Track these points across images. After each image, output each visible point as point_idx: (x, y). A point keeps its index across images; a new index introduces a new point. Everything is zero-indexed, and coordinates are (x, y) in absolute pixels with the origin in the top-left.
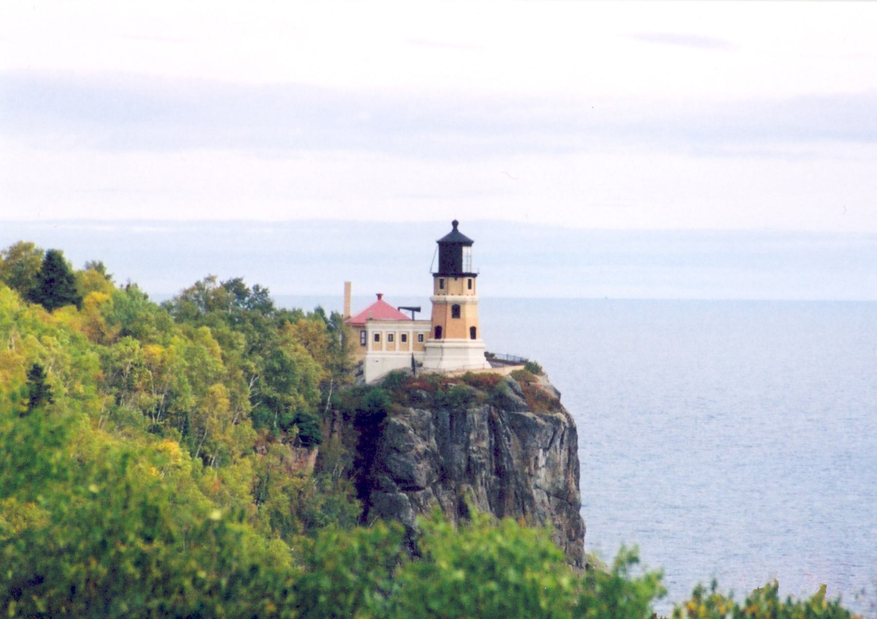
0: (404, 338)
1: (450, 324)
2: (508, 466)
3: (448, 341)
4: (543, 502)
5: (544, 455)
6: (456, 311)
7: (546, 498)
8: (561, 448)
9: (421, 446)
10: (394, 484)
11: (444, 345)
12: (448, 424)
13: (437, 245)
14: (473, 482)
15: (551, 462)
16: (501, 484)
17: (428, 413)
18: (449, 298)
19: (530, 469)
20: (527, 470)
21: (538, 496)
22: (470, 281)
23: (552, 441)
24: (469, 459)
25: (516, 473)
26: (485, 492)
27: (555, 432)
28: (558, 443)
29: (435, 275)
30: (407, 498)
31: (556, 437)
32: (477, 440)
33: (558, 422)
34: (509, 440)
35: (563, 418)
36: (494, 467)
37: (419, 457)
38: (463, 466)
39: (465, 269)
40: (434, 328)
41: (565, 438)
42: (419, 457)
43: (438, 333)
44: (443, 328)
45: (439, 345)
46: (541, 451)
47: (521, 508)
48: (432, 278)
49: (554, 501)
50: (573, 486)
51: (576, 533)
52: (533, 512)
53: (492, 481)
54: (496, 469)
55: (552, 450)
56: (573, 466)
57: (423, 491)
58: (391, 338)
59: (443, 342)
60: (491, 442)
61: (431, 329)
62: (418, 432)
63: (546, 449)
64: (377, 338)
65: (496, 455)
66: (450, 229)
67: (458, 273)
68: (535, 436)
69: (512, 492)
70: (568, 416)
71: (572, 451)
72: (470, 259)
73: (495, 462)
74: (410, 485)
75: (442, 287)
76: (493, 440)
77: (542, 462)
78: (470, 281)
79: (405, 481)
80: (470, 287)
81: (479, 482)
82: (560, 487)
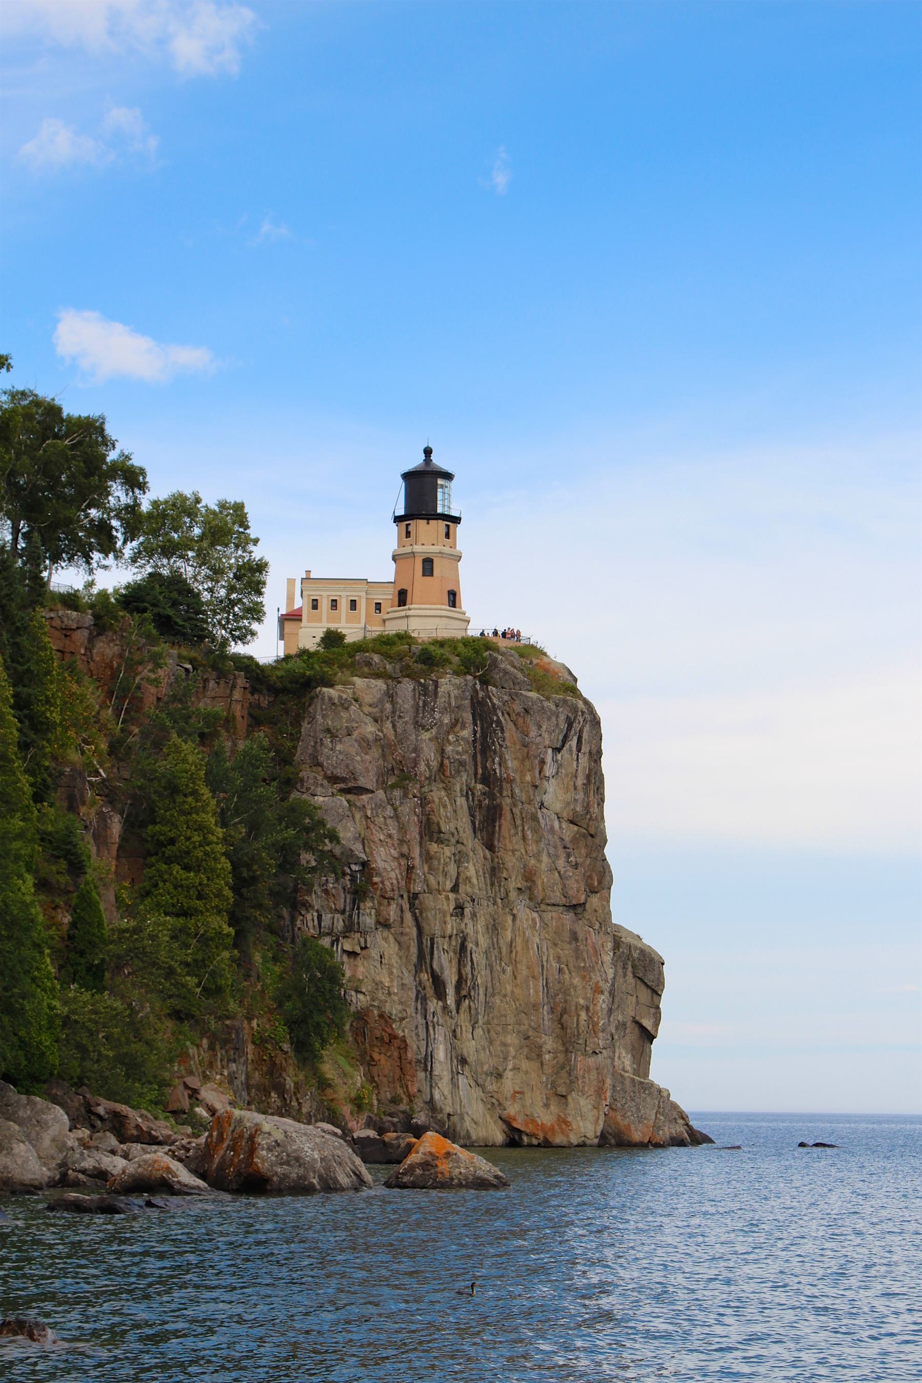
0: (353, 605)
1: (420, 585)
2: (500, 771)
3: (413, 608)
4: (552, 827)
5: (555, 761)
6: (428, 566)
7: (556, 825)
8: (579, 750)
9: (369, 729)
10: (325, 782)
15: (563, 771)
16: (491, 795)
17: (380, 685)
18: (418, 548)
20: (528, 778)
21: (547, 819)
22: (448, 526)
23: (565, 739)
25: (511, 781)
26: (465, 807)
28: (574, 742)
29: (398, 519)
31: (573, 732)
33: (575, 709)
35: (581, 704)
36: (480, 771)
37: (365, 744)
38: (435, 764)
39: (440, 510)
40: (397, 593)
41: (585, 736)
43: (402, 598)
45: (403, 614)
46: (550, 751)
47: (520, 834)
49: (569, 831)
50: (595, 809)
51: (600, 882)
52: (538, 842)
53: (478, 793)
54: (483, 774)
57: (370, 795)
58: (334, 604)
59: (410, 609)
60: (475, 732)
61: (393, 595)
62: (367, 709)
67: (433, 515)
69: (508, 808)
70: (586, 702)
71: (596, 755)
73: (482, 763)
74: (350, 785)
78: (448, 526)
79: (343, 780)
80: (447, 536)
82: (578, 809)
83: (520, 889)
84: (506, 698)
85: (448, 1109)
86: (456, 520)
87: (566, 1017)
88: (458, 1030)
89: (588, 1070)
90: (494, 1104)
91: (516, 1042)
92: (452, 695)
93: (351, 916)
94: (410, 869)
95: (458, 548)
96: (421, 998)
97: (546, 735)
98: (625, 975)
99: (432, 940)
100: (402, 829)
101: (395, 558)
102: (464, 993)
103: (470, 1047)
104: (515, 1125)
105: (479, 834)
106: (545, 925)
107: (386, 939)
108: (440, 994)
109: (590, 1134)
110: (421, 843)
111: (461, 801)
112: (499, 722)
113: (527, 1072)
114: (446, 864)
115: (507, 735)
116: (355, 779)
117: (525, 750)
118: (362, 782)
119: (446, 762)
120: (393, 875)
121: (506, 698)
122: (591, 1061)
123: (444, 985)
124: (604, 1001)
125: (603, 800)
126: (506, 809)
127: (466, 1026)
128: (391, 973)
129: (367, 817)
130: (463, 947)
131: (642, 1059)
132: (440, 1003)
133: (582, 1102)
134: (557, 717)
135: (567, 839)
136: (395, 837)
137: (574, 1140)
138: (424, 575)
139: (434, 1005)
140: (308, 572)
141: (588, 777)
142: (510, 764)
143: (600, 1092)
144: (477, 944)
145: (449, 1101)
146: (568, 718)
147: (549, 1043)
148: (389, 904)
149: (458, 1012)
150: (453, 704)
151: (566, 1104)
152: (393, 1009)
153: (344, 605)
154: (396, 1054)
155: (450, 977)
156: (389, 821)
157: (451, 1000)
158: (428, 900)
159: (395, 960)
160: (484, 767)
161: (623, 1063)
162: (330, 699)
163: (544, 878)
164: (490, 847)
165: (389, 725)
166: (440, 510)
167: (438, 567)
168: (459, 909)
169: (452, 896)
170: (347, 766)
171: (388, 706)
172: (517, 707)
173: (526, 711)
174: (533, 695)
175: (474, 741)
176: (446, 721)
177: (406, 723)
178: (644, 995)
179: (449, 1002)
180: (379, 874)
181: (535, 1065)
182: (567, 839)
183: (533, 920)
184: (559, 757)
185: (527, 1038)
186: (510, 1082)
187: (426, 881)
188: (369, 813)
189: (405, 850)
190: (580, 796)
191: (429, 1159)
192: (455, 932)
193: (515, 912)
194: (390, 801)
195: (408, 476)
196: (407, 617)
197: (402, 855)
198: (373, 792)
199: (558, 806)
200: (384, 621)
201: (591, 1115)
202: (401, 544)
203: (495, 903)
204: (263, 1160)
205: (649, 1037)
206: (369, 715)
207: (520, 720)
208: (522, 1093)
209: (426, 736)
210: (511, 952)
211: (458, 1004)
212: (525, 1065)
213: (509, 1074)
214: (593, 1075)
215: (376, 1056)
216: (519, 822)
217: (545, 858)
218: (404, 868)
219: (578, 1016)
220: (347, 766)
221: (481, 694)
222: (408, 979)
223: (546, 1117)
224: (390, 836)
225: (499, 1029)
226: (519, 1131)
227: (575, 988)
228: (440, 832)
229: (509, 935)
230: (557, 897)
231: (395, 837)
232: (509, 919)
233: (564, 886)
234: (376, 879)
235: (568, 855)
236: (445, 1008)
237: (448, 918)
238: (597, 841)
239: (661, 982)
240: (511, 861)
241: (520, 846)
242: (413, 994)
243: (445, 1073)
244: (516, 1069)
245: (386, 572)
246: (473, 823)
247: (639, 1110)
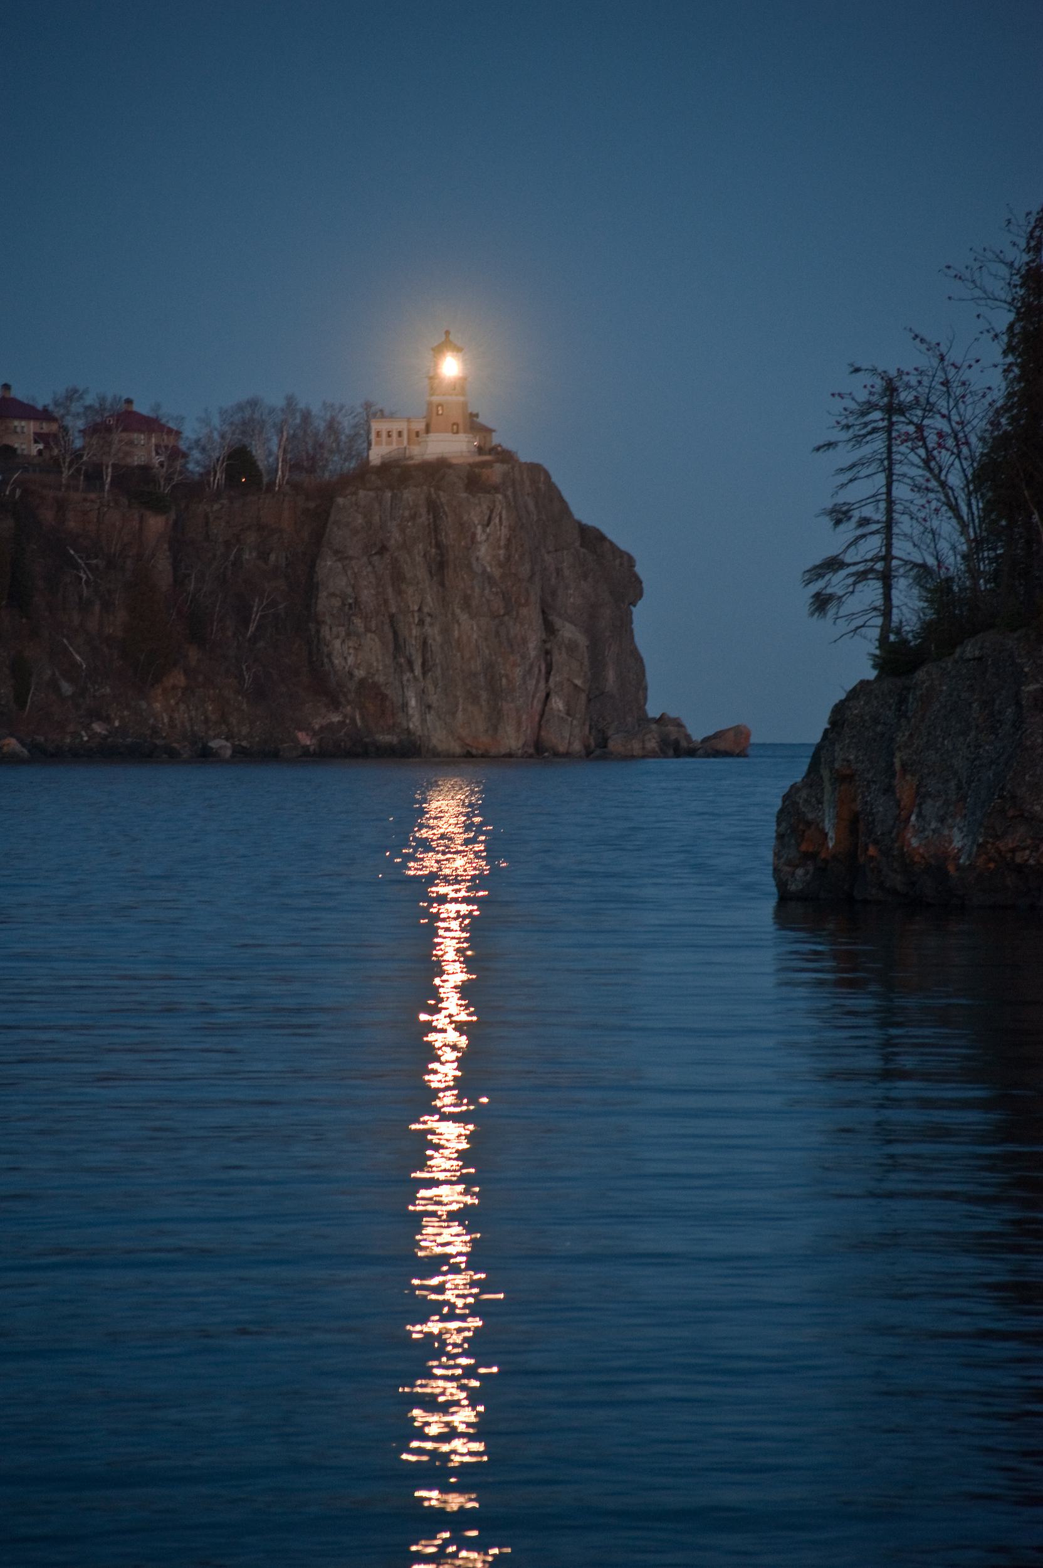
3: (432, 436)
8: (501, 524)
11: (428, 439)
12: (389, 503)
17: (372, 494)
20: (463, 543)
27: (492, 511)
28: (497, 520)
31: (494, 514)
32: (413, 517)
34: (447, 518)
36: (433, 541)
41: (504, 516)
46: (479, 527)
49: (497, 573)
54: (436, 542)
58: (389, 435)
60: (429, 519)
65: (436, 531)
76: (431, 516)
77: (480, 537)
81: (416, 551)
85: (418, 733)
88: (426, 690)
92: (410, 499)
94: (386, 601)
98: (560, 654)
99: (404, 639)
102: (426, 669)
103: (433, 698)
104: (467, 742)
105: (435, 578)
108: (412, 671)
111: (418, 559)
112: (445, 513)
115: (449, 519)
118: (351, 553)
122: (512, 705)
124: (520, 671)
127: (431, 688)
130: (425, 643)
132: (412, 675)
137: (503, 751)
139: (408, 675)
142: (451, 536)
143: (519, 723)
144: (434, 640)
145: (419, 728)
146: (489, 507)
147: (484, 695)
148: (370, 621)
149: (424, 679)
150: (411, 503)
152: (380, 679)
157: (418, 671)
160: (436, 538)
161: (558, 706)
164: (442, 584)
168: (421, 623)
174: (464, 495)
175: (429, 525)
179: (416, 674)
183: (472, 625)
184: (488, 530)
188: (356, 570)
190: (502, 552)
192: (418, 634)
193: (460, 621)
194: (370, 563)
200: (420, 442)
203: (446, 616)
209: (395, 523)
210: (459, 645)
211: (424, 674)
217: (477, 590)
219: (501, 680)
221: (434, 496)
224: (370, 582)
229: (456, 633)
232: (456, 626)
234: (362, 607)
235: (491, 588)
236: (415, 677)
237: (413, 626)
242: (392, 670)
243: (416, 713)
246: (430, 572)
247: (561, 734)
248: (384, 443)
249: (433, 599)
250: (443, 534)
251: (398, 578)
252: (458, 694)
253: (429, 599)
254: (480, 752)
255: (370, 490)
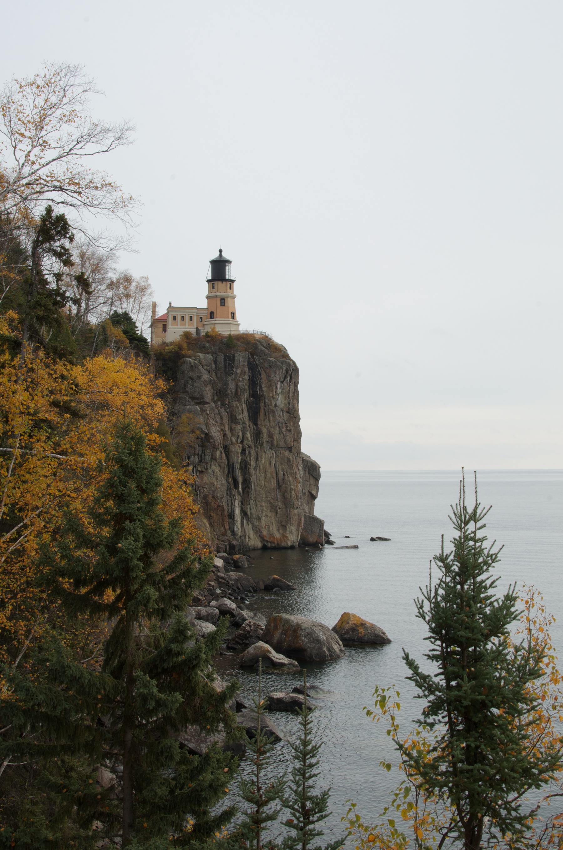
0: (191, 318)
1: (219, 310)
3: (218, 320)
4: (280, 415)
6: (223, 301)
10: (190, 400)
11: (216, 322)
12: (223, 364)
13: (209, 264)
14: (239, 401)
17: (210, 356)
18: (218, 294)
19: (273, 394)
20: (271, 395)
22: (230, 284)
24: (237, 385)
28: (289, 379)
29: (209, 281)
30: (199, 409)
35: (291, 363)
36: (251, 392)
37: (206, 384)
38: (233, 390)
39: (227, 277)
42: (206, 384)
43: (212, 315)
44: (215, 312)
45: (213, 322)
46: (279, 383)
48: (207, 284)
49: (286, 416)
51: (297, 436)
55: (285, 382)
56: (296, 393)
60: (249, 376)
63: (282, 382)
64: (175, 318)
66: (218, 254)
68: (276, 373)
72: (231, 272)
75: (213, 288)
78: (230, 284)
79: (197, 399)
80: (230, 288)
81: (243, 400)
83: (268, 442)
84: (262, 361)
86: (233, 281)
87: (286, 494)
89: (295, 515)
90: (258, 531)
91: (266, 504)
93: (201, 456)
95: (235, 293)
96: (229, 489)
97: (278, 376)
100: (221, 418)
101: (207, 297)
104: (265, 539)
106: (277, 456)
107: (215, 465)
109: (295, 541)
110: (228, 425)
112: (259, 372)
113: (270, 517)
114: (239, 432)
115: (262, 377)
116: (203, 398)
117: (269, 383)
119: (239, 389)
120: (218, 438)
121: (262, 361)
123: (238, 483)
125: (298, 402)
126: (262, 408)
128: (217, 479)
129: (207, 414)
131: (312, 506)
133: (292, 528)
134: (283, 369)
135: (285, 419)
136: (219, 422)
138: (221, 305)
140: (170, 303)
141: (294, 393)
151: (286, 529)
153: (187, 318)
154: (220, 513)
155: (240, 480)
156: (216, 416)
158: (232, 448)
159: (219, 474)
162: (190, 363)
163: (276, 436)
164: (256, 424)
165: (214, 374)
166: (227, 277)
167: (229, 302)
169: (241, 445)
170: (199, 393)
171: (214, 365)
172: (266, 365)
173: (270, 366)
176: (238, 372)
177: (221, 373)
178: (312, 481)
180: (213, 438)
181: (274, 514)
182: (285, 419)
184: (282, 385)
185: (271, 503)
186: (264, 521)
187: (231, 440)
188: (208, 412)
189: (223, 427)
191: (354, 626)
195: (213, 262)
196: (215, 324)
197: (222, 430)
198: (209, 403)
199: (282, 406)
200: (204, 325)
201: (295, 533)
202: (210, 291)
204: (303, 641)
205: (314, 497)
206: (206, 370)
207: (268, 371)
208: (269, 526)
212: (269, 514)
213: (264, 518)
214: (297, 517)
215: (212, 515)
216: (267, 414)
218: (222, 435)
219: (291, 493)
220: (199, 393)
221: (252, 359)
222: (224, 482)
223: (277, 535)
224: (217, 422)
225: (260, 500)
226: (267, 541)
227: (290, 481)
228: (236, 419)
230: (282, 444)
231: (219, 422)
233: (285, 440)
235: (287, 427)
236: (239, 492)
238: (297, 420)
239: (319, 476)
240: (264, 431)
241: (268, 424)
244: (266, 516)
245: (203, 304)
247: (312, 529)
248: (179, 323)
249: (251, 435)
250: (258, 387)
251: (233, 419)
252: (263, 504)
253: (248, 435)
254: (273, 545)
255: (208, 353)
